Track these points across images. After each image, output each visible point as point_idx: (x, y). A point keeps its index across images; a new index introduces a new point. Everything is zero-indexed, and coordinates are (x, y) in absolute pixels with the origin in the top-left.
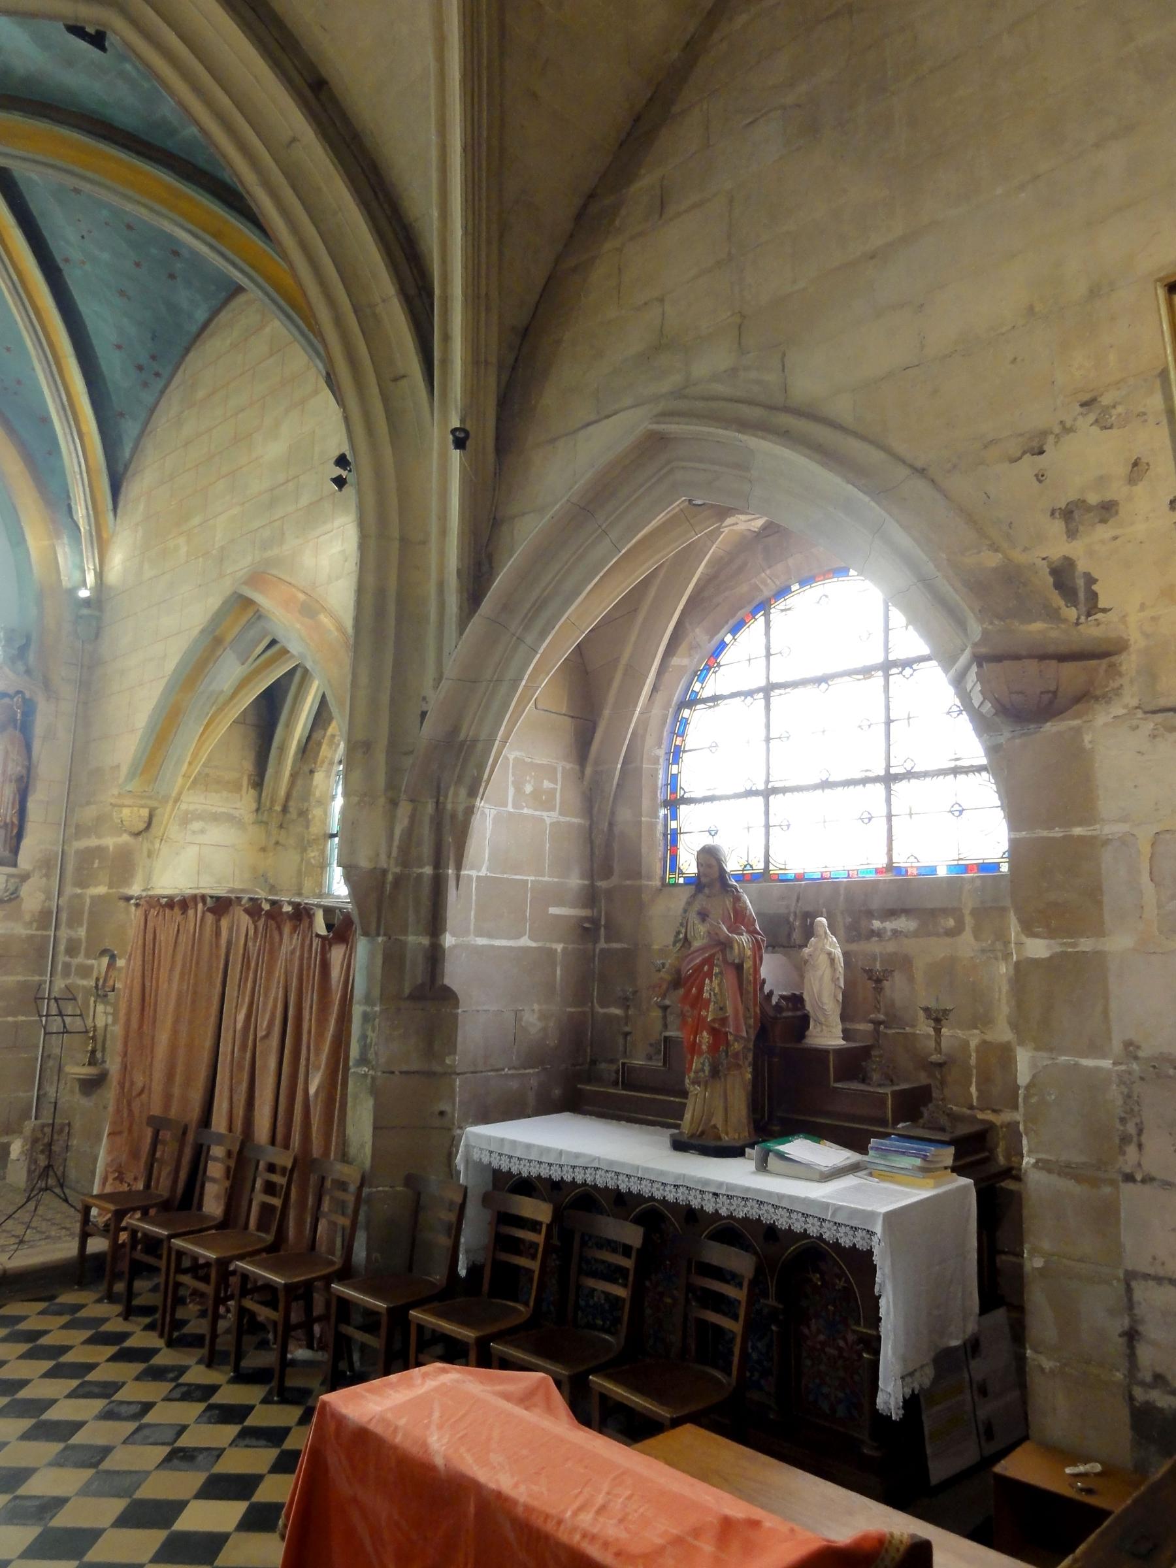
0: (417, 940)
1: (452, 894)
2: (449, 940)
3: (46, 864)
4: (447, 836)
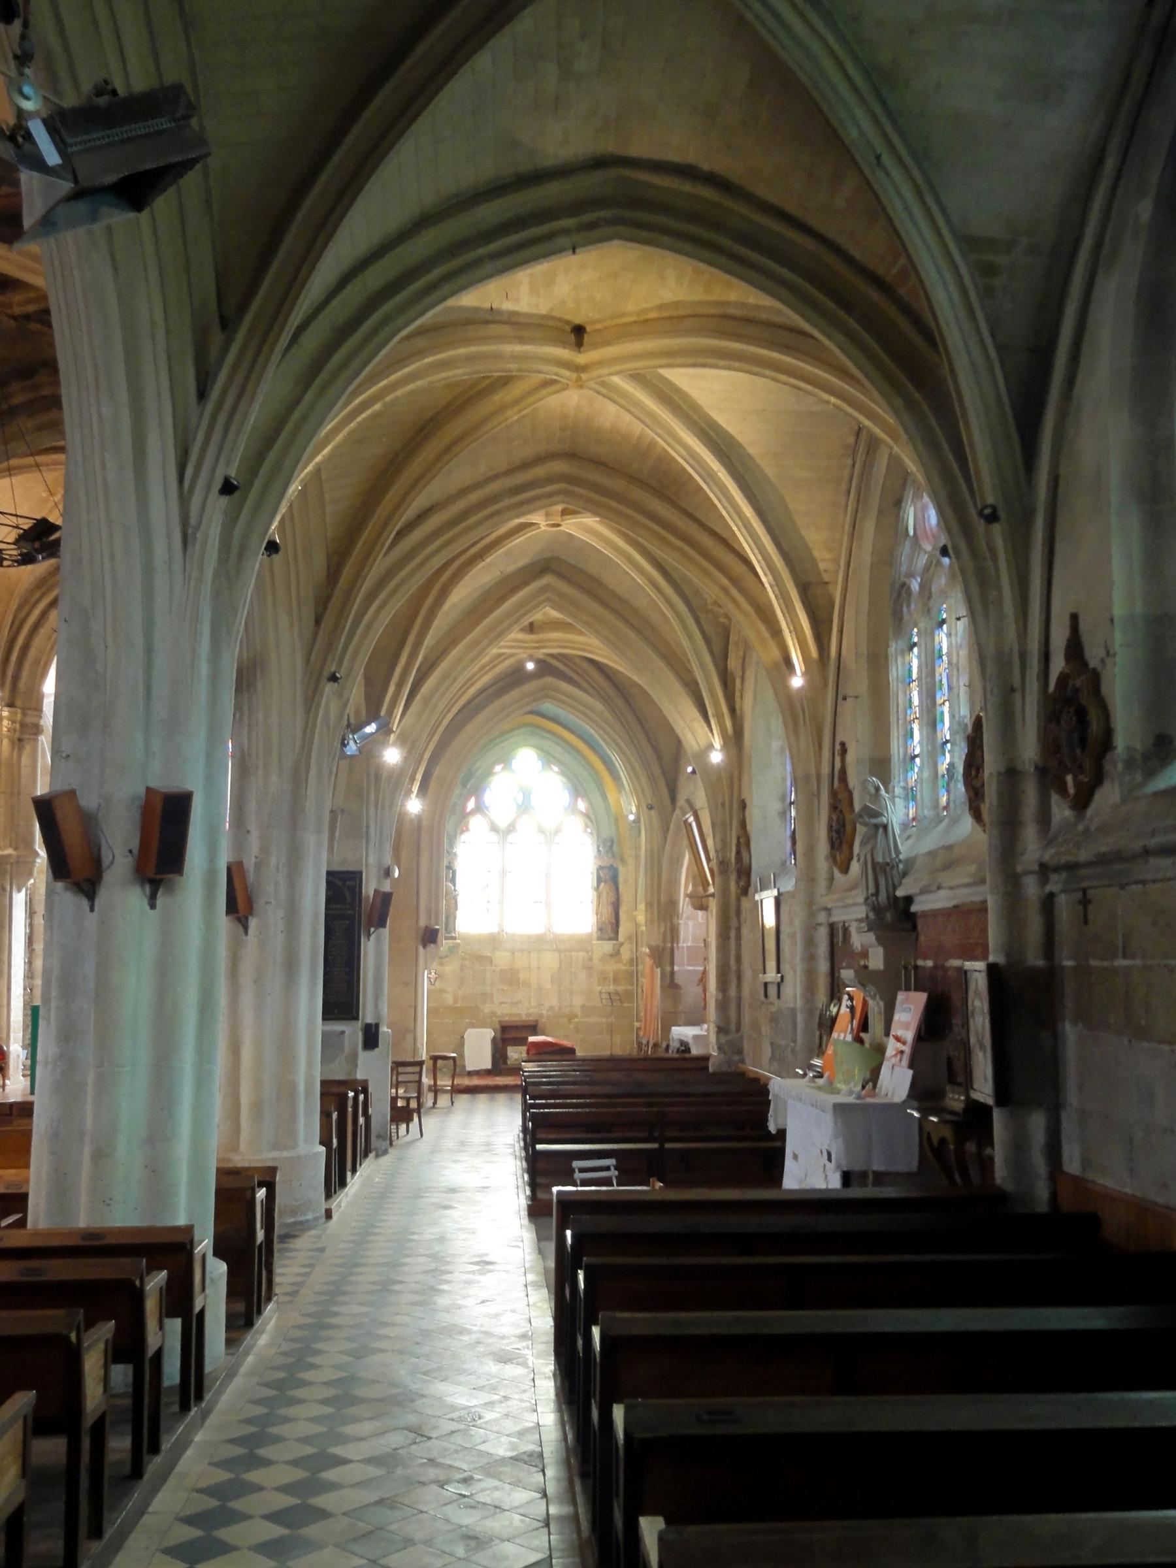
0: (668, 969)
1: (676, 953)
2: (676, 968)
3: (629, 938)
4: (673, 933)
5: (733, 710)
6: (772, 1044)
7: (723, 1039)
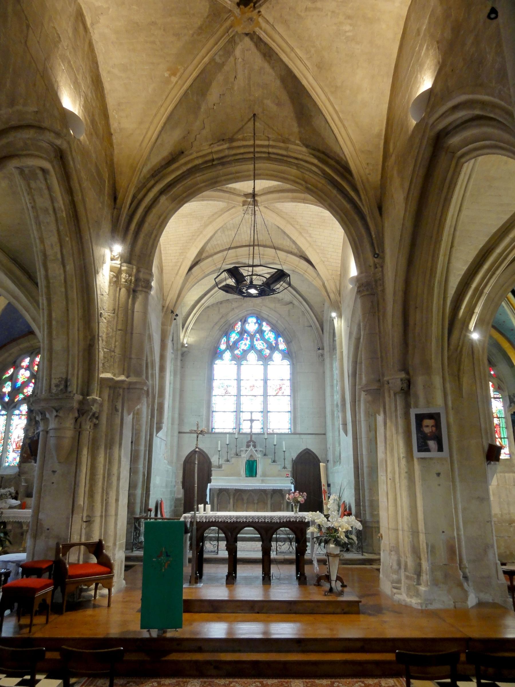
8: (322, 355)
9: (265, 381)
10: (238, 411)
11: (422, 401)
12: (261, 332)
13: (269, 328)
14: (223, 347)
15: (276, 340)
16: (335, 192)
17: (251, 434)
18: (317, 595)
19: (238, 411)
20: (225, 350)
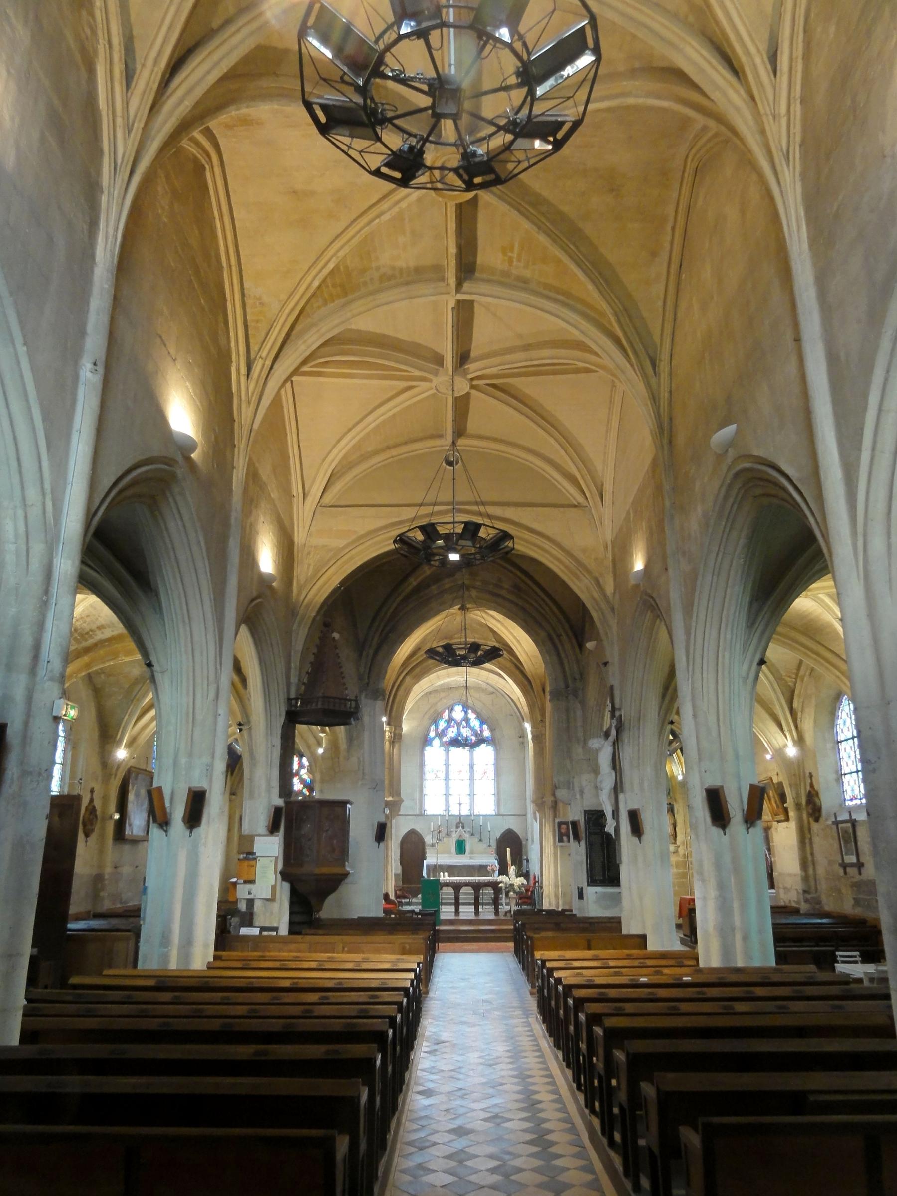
3: (683, 843)
5: (796, 727)
6: (854, 899)
7: (808, 896)
8: (523, 743)
9: (472, 767)
10: (447, 795)
11: (561, 815)
12: (467, 719)
13: (475, 716)
14: (432, 734)
15: (481, 727)
16: (518, 672)
17: (460, 816)
18: (502, 917)
19: (447, 795)
20: (434, 738)
